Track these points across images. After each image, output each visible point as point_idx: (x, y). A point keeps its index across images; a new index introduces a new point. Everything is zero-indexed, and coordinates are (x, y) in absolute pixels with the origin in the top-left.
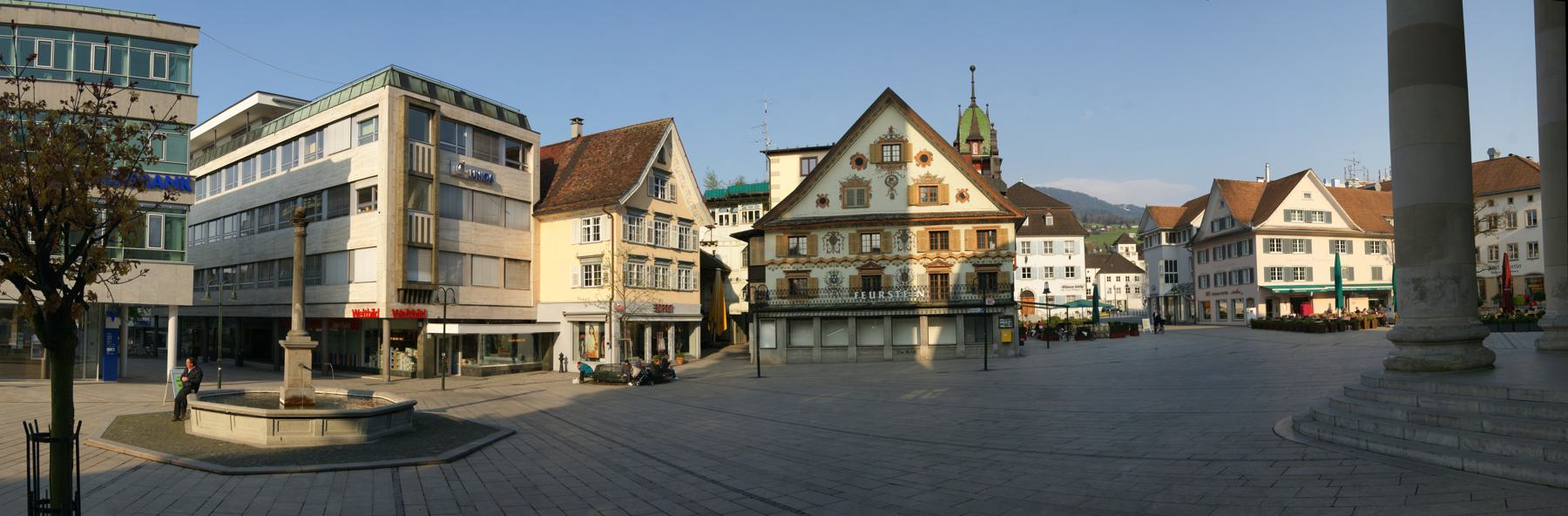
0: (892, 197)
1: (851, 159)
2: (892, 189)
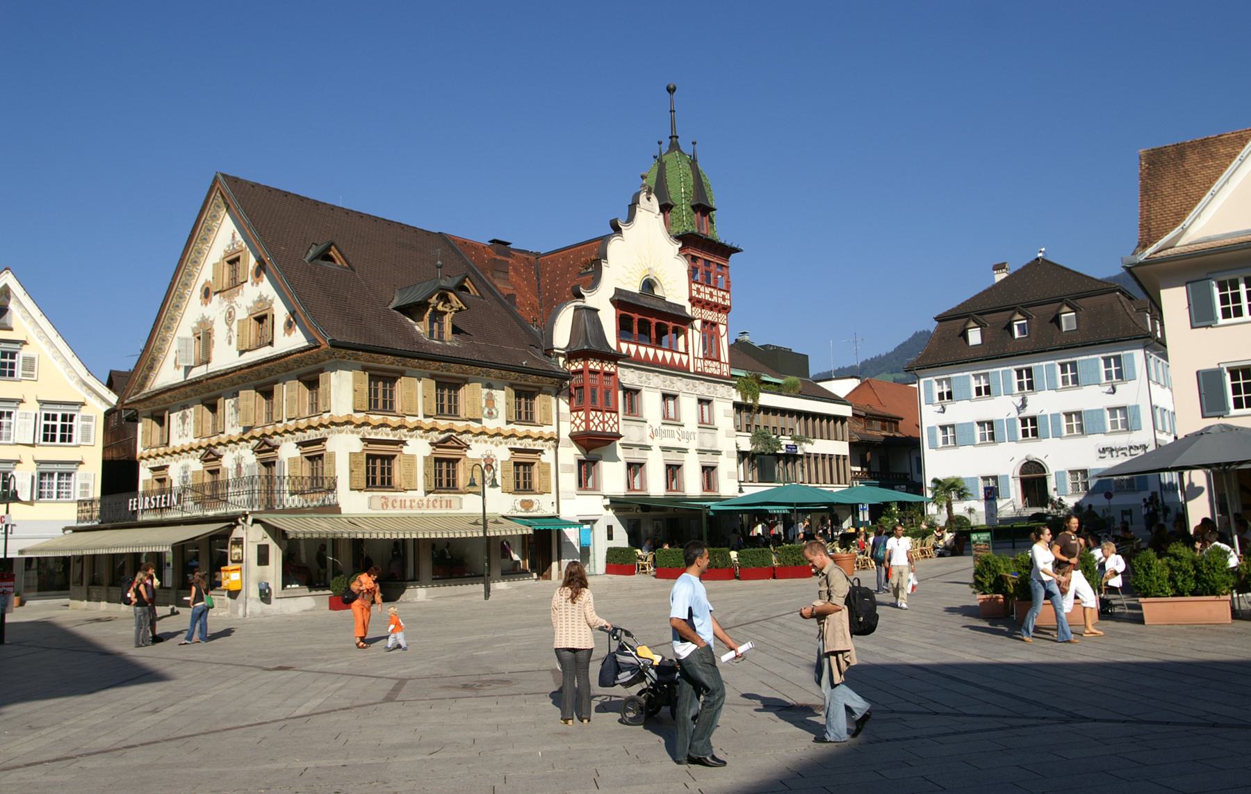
0: (230, 343)
1: (201, 291)
2: (230, 329)
